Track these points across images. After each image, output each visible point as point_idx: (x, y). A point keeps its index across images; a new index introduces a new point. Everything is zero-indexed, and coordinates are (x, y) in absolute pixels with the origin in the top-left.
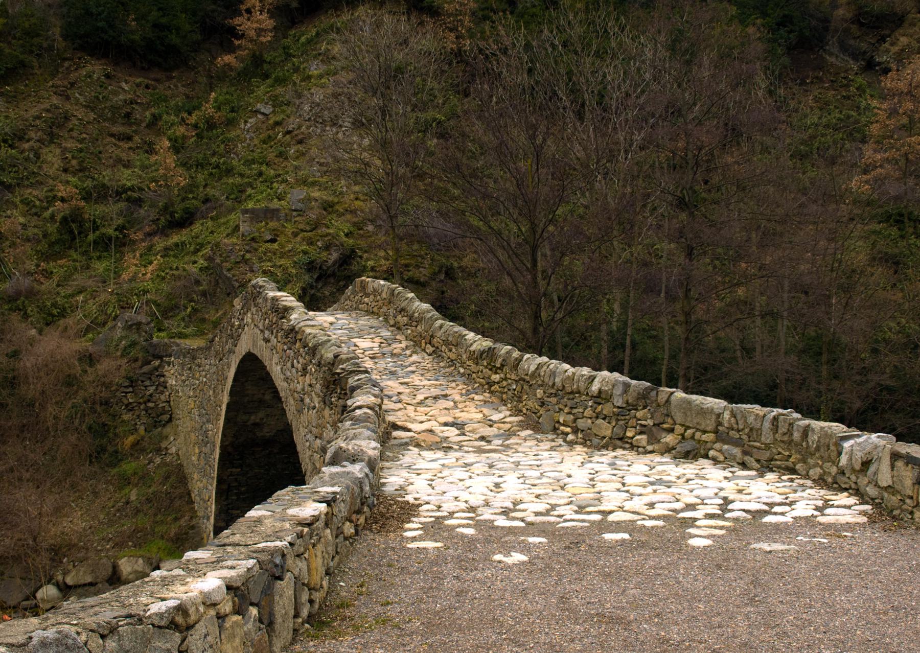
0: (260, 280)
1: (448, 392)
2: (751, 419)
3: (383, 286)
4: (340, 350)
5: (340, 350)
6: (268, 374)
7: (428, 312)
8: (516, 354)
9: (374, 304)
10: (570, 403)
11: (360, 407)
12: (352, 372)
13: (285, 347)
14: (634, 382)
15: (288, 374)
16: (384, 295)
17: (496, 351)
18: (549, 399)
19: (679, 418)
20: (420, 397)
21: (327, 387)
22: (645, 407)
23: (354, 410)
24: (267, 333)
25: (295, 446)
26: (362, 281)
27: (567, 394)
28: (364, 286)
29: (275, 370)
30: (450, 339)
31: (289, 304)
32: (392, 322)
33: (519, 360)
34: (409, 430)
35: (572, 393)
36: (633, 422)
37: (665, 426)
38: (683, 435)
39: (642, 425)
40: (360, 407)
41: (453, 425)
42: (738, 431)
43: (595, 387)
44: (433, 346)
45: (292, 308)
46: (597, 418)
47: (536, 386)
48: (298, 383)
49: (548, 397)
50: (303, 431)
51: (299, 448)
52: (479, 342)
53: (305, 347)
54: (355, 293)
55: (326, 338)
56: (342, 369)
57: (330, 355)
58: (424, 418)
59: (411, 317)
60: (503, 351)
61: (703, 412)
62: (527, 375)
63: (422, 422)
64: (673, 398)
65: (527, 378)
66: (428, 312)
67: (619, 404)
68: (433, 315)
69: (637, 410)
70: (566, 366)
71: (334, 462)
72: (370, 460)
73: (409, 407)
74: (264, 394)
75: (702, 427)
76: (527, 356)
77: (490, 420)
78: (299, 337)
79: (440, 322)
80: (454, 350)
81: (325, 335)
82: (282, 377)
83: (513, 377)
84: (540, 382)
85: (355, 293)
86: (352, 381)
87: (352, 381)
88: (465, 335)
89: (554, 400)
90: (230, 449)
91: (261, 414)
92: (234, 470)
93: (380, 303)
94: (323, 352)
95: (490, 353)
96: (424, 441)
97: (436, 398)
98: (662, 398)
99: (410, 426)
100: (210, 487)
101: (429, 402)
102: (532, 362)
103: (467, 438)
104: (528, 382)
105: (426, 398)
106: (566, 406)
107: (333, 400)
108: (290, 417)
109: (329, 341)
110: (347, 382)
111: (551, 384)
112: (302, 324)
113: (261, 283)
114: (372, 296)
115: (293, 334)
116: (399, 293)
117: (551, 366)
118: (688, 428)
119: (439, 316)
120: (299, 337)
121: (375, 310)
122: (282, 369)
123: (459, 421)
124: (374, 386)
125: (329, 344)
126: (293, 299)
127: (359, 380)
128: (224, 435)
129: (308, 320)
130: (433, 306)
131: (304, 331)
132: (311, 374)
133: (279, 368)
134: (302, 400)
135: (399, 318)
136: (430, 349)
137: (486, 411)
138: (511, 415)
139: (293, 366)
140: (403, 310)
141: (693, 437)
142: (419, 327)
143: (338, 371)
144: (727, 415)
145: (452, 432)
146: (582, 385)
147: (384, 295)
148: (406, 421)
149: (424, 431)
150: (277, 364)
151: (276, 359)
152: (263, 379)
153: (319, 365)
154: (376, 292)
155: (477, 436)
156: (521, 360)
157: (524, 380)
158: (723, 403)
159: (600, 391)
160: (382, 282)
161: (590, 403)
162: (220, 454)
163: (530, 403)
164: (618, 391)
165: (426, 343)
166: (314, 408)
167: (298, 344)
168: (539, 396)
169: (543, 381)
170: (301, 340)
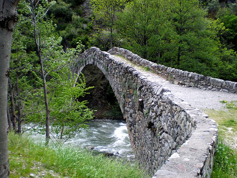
2: (230, 84)
10: (183, 79)
14: (200, 75)
19: (211, 83)
22: (203, 80)
27: (181, 77)
35: (183, 76)
36: (199, 83)
37: (208, 85)
38: (213, 87)
39: (202, 84)
42: (227, 86)
43: (190, 75)
46: (190, 82)
61: (218, 82)
64: (210, 79)
67: (197, 79)
69: (201, 81)
70: (181, 71)
75: (218, 85)
76: (169, 68)
79: (141, 59)
89: (178, 78)
95: (158, 67)
98: (208, 79)
106: (182, 79)
112: (113, 59)
114: (119, 52)
117: (177, 71)
118: (214, 85)
131: (114, 60)
141: (215, 87)
144: (224, 83)
146: (186, 75)
154: (120, 51)
158: (223, 81)
159: (191, 77)
161: (189, 79)
164: (196, 77)
168: (173, 77)
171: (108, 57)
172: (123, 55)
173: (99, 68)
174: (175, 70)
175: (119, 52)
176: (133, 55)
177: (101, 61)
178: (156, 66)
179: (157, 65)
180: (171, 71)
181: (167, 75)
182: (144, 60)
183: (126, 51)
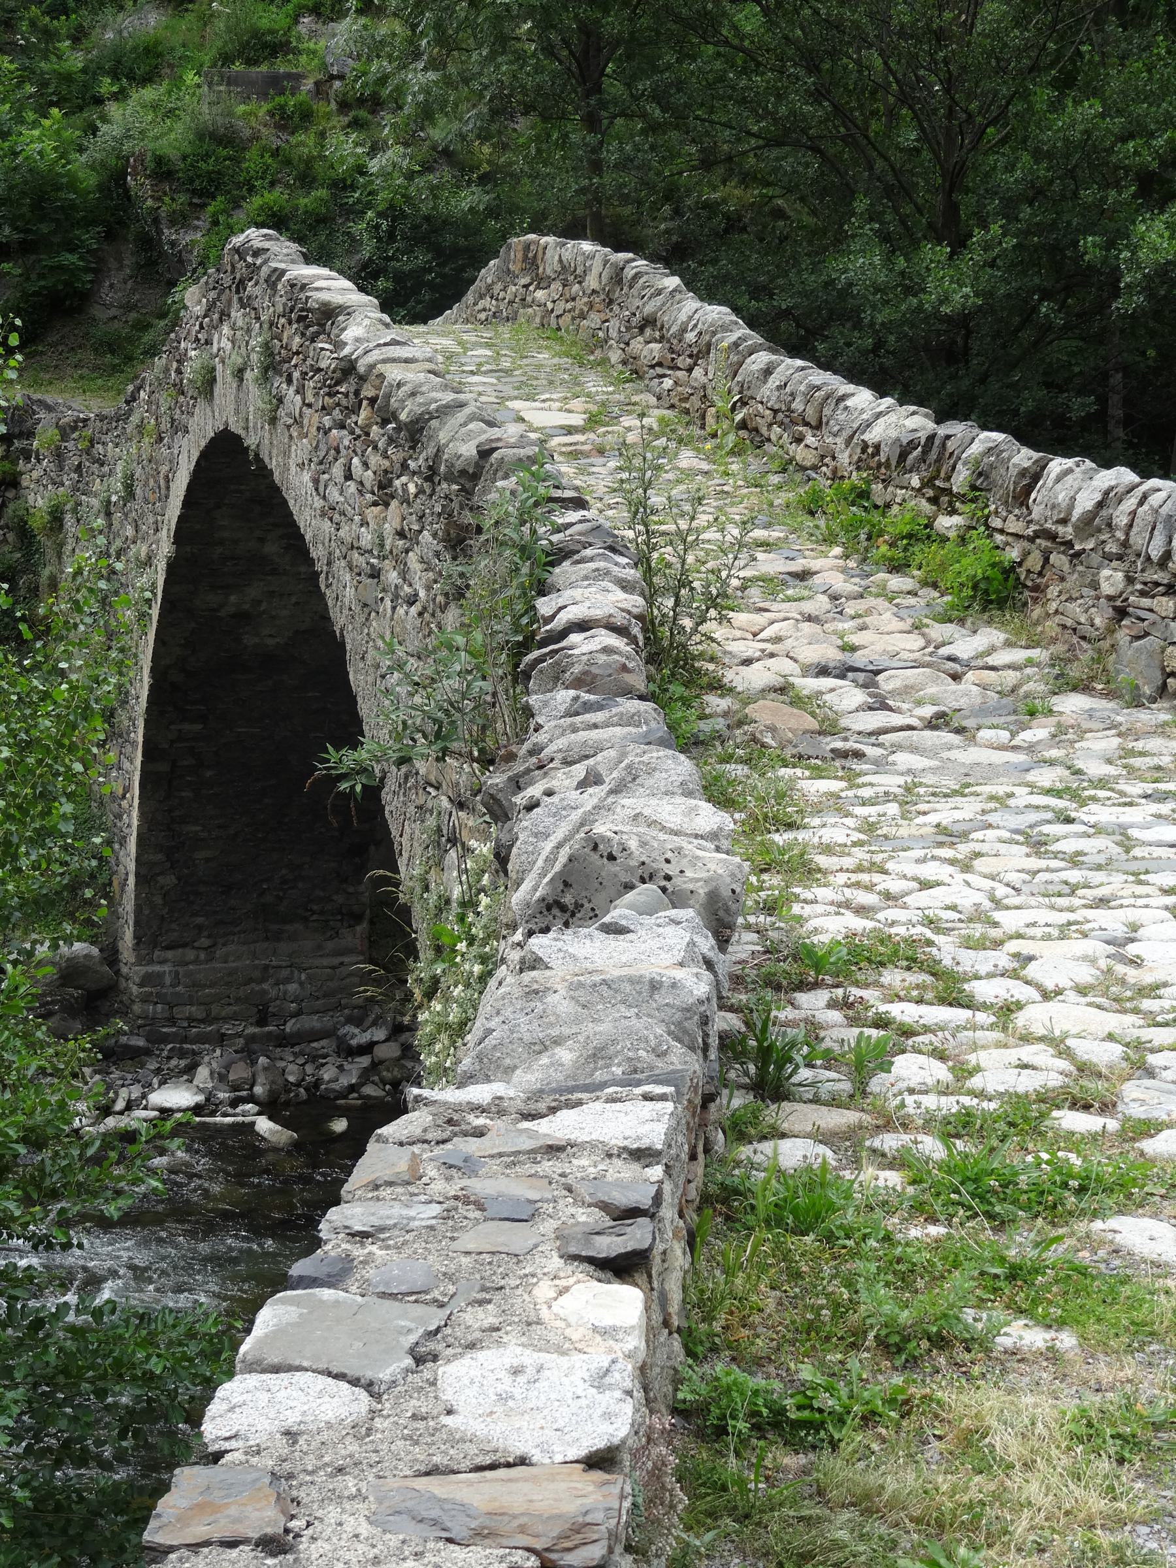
0: (254, 236)
1: (815, 564)
4: (494, 433)
5: (494, 433)
6: (277, 490)
7: (725, 328)
8: (1024, 457)
9: (561, 306)
11: (583, 626)
13: (327, 421)
15: (334, 495)
16: (592, 282)
17: (951, 445)
18: (1146, 602)
23: (564, 634)
26: (527, 247)
28: (531, 261)
30: (798, 405)
31: (337, 299)
33: (1034, 476)
40: (583, 626)
41: (844, 671)
47: (1096, 559)
48: (364, 523)
49: (1143, 594)
52: (892, 418)
53: (384, 422)
54: (507, 275)
55: (448, 397)
57: (468, 450)
58: (750, 648)
59: (673, 344)
60: (976, 448)
62: (1064, 521)
63: (747, 662)
65: (1066, 532)
66: (725, 328)
68: (742, 339)
71: (564, 907)
72: (713, 897)
74: (262, 540)
76: (1057, 465)
77: (951, 659)
78: (368, 392)
79: (762, 358)
80: (810, 440)
81: (445, 387)
82: (318, 503)
83: (1013, 526)
84: (1112, 548)
92: (186, 727)
93: (581, 303)
94: (443, 437)
95: (929, 456)
100: (126, 765)
102: (1076, 484)
103: (897, 720)
104: (1069, 544)
108: (339, 619)
109: (462, 405)
111: (1155, 553)
113: (257, 244)
114: (556, 286)
116: (637, 276)
117: (1155, 500)
119: (761, 340)
120: (368, 392)
122: (316, 481)
123: (859, 659)
124: (613, 549)
125: (462, 415)
126: (348, 284)
130: (736, 310)
131: (381, 376)
132: (406, 501)
133: (306, 477)
134: (375, 574)
135: (637, 345)
137: (938, 631)
138: (1008, 644)
139: (348, 477)
140: (649, 322)
142: (698, 372)
145: (846, 697)
147: (592, 282)
150: (301, 466)
153: (431, 475)
154: (569, 274)
155: (928, 711)
156: (1036, 477)
157: (1052, 537)
160: (587, 246)
162: (152, 688)
163: (1075, 608)
166: (412, 601)
167: (364, 413)
168: (1107, 589)
169: (1125, 544)
170: (373, 401)
171: (339, 345)
173: (277, 476)
174: (1130, 503)
175: (556, 286)
176: (683, 317)
178: (912, 445)
179: (931, 425)
180: (1077, 513)
181: (1034, 561)
182: (789, 365)
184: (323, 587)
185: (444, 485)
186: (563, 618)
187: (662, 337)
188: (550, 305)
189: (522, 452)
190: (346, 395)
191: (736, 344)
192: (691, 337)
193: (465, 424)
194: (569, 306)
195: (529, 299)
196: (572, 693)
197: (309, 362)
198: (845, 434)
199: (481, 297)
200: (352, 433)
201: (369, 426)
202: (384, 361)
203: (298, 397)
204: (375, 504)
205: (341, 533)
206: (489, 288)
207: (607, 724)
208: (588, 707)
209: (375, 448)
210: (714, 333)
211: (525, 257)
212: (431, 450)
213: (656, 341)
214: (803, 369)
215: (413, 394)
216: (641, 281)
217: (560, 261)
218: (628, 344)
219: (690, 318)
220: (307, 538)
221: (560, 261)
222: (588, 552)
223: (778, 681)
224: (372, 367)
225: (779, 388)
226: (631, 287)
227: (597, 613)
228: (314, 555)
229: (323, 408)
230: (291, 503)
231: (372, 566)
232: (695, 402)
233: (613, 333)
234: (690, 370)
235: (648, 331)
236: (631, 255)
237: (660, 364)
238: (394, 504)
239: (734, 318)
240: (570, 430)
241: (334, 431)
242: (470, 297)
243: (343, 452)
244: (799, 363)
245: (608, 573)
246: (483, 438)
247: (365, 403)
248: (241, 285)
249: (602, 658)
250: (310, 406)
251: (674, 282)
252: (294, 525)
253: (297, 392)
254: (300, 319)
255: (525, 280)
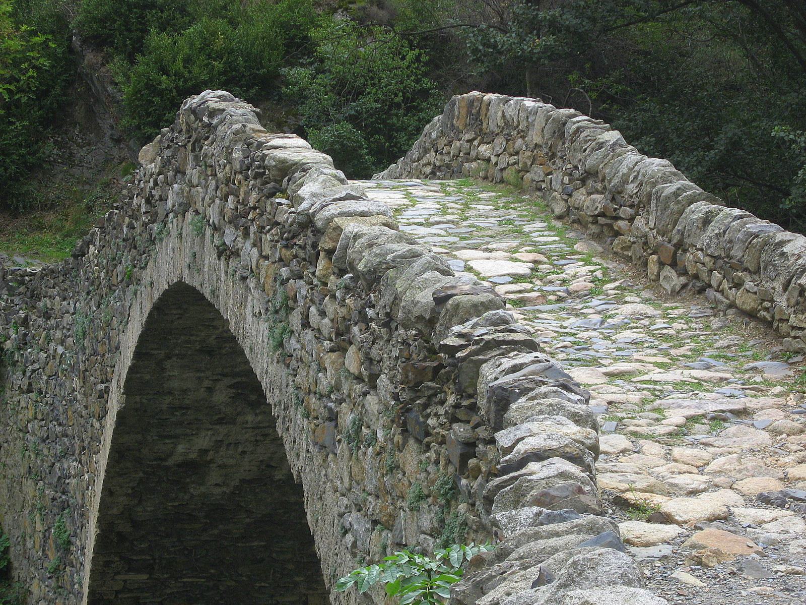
3: (535, 112)
4: (447, 281)
5: (447, 281)
6: (234, 339)
7: (665, 179)
9: (505, 160)
11: (539, 456)
12: (491, 345)
13: (284, 272)
16: (535, 137)
20: (676, 417)
21: (415, 387)
23: (522, 462)
24: (230, 236)
25: (311, 540)
26: (471, 103)
28: (476, 115)
29: (254, 334)
30: (737, 252)
32: (559, 208)
34: (666, 519)
40: (539, 456)
44: (684, 272)
45: (303, 168)
48: (322, 369)
50: (335, 503)
51: (322, 547)
53: (341, 273)
54: (451, 132)
55: (402, 248)
56: (461, 336)
57: (425, 297)
58: (696, 481)
59: (615, 195)
63: (694, 493)
66: (665, 179)
73: (648, 446)
74: (210, 390)
78: (325, 243)
79: (702, 207)
80: (749, 284)
81: (401, 238)
85: (451, 132)
86: (494, 373)
87: (494, 373)
88: (782, 243)
90: (124, 527)
91: (203, 441)
92: (132, 576)
93: (524, 158)
94: (400, 286)
96: (717, 554)
97: (718, 419)
99: (669, 505)
101: (700, 431)
105: (692, 419)
107: (431, 422)
109: (416, 255)
110: (477, 374)
112: (333, 209)
113: (214, 104)
114: (500, 141)
115: (308, 237)
116: (579, 130)
119: (699, 190)
120: (325, 243)
121: (509, 174)
125: (417, 265)
127: (515, 369)
128: (108, 491)
129: (349, 197)
131: (338, 229)
134: (333, 417)
136: (672, 279)
139: (306, 324)
142: (639, 222)
143: (451, 341)
147: (535, 137)
148: (649, 490)
149: (711, 520)
151: (255, 302)
152: (210, 353)
153: (389, 322)
154: (511, 129)
160: (529, 103)
165: (661, 264)
167: (322, 263)
170: (330, 253)
171: (295, 200)
172: (536, 173)
173: (232, 325)
176: (624, 169)
177: (248, 245)
183: (561, 125)
184: (279, 431)
185: (401, 331)
186: (522, 447)
187: (605, 188)
188: (494, 159)
189: (475, 299)
190: (303, 247)
191: (676, 194)
192: (631, 188)
193: (421, 273)
194: (513, 159)
195: (473, 153)
196: (535, 509)
197: (266, 216)
198: (782, 279)
199: (426, 151)
200: (310, 283)
201: (327, 276)
202: (341, 215)
203: (255, 250)
204: (332, 350)
205: (298, 379)
206: (434, 143)
207: (568, 533)
208: (551, 519)
209: (333, 297)
210: (654, 184)
211: (469, 113)
212: (387, 299)
213: (597, 192)
214: (741, 217)
215: (370, 246)
216: (583, 135)
217: (504, 116)
218: (570, 195)
219: (631, 170)
220: (263, 384)
221: (504, 116)
222: (543, 389)
223: (720, 510)
224: (330, 220)
225: (718, 235)
226: (572, 141)
227: (554, 444)
228: (270, 400)
229: (281, 260)
230: (247, 351)
231: (330, 410)
232: (638, 249)
233: (556, 186)
234: (631, 219)
235: (590, 183)
236: (572, 111)
237: (602, 214)
238: (352, 350)
239: (674, 170)
240: (516, 278)
241: (291, 281)
242: (415, 152)
243: (301, 302)
244: (737, 212)
245: (560, 408)
246: (438, 286)
247: (322, 254)
248: (197, 145)
249: (561, 483)
250: (266, 258)
251: (614, 136)
252: (250, 373)
253: (254, 245)
254: (257, 176)
255: (467, 137)
